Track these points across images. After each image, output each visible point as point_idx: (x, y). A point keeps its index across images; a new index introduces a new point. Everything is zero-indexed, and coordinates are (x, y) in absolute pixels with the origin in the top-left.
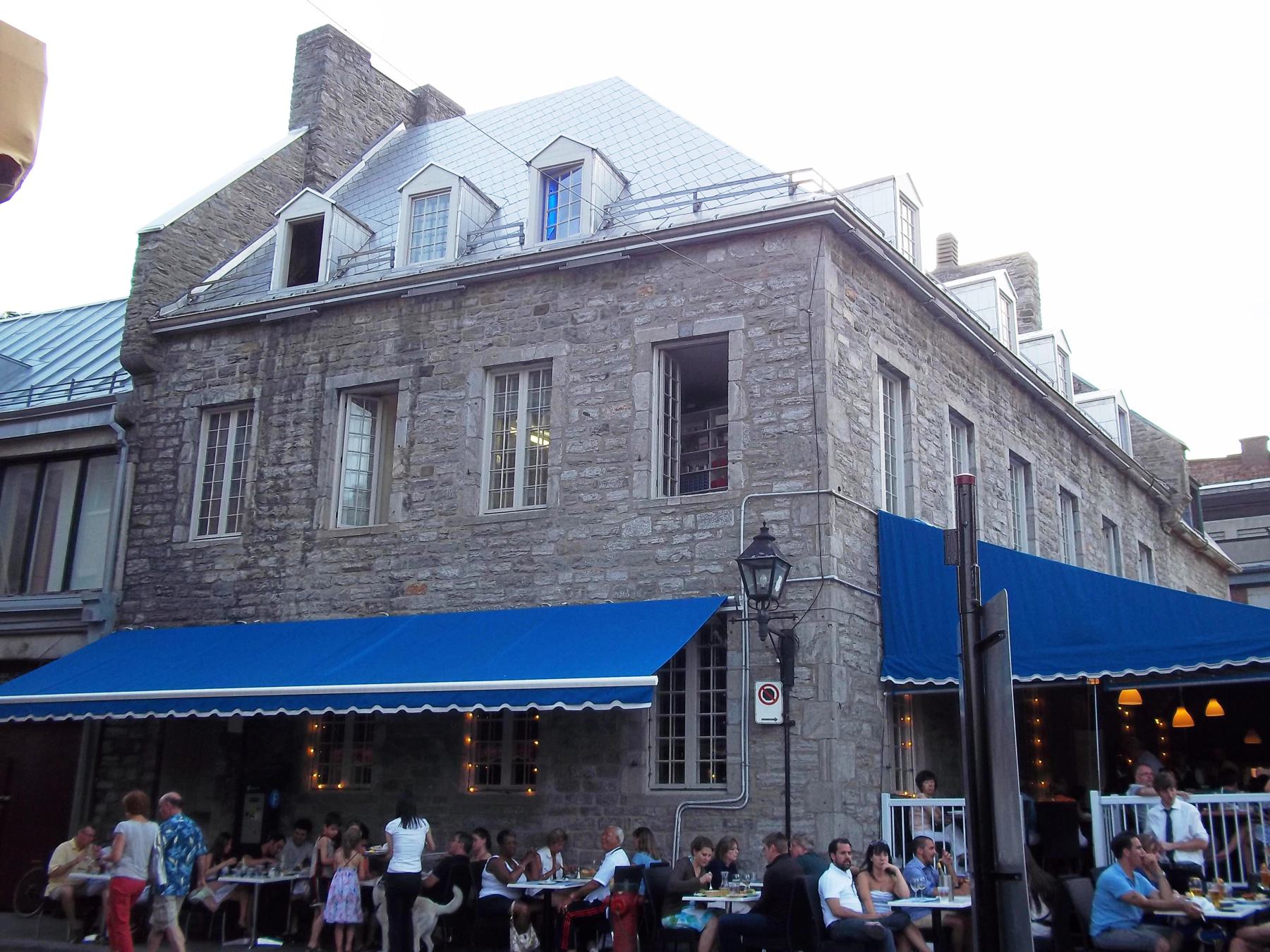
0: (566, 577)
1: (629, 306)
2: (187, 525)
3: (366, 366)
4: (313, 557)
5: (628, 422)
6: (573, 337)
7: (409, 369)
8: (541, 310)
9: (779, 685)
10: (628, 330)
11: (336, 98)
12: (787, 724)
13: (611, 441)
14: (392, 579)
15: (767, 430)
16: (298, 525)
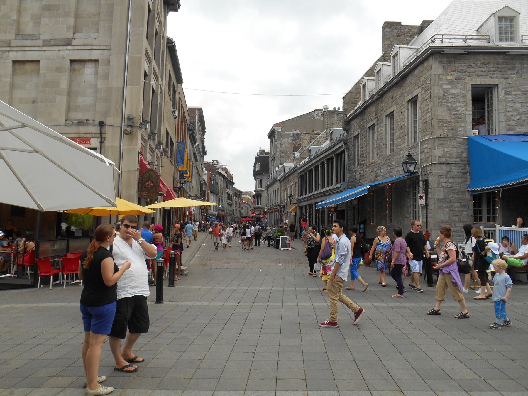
0: (397, 169)
1: (404, 91)
2: (354, 165)
3: (371, 121)
4: (367, 170)
5: (404, 125)
6: (397, 104)
7: (376, 120)
8: (392, 98)
9: (424, 195)
10: (404, 100)
11: (390, 41)
12: (427, 205)
13: (402, 131)
14: (377, 174)
15: (425, 121)
16: (365, 162)
